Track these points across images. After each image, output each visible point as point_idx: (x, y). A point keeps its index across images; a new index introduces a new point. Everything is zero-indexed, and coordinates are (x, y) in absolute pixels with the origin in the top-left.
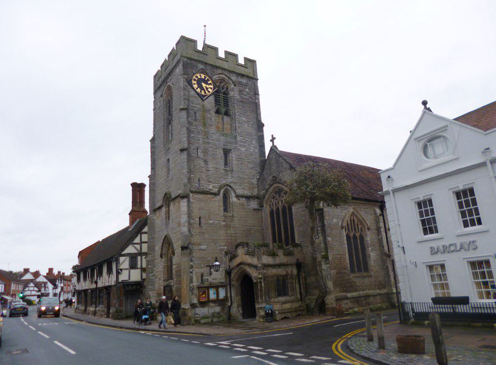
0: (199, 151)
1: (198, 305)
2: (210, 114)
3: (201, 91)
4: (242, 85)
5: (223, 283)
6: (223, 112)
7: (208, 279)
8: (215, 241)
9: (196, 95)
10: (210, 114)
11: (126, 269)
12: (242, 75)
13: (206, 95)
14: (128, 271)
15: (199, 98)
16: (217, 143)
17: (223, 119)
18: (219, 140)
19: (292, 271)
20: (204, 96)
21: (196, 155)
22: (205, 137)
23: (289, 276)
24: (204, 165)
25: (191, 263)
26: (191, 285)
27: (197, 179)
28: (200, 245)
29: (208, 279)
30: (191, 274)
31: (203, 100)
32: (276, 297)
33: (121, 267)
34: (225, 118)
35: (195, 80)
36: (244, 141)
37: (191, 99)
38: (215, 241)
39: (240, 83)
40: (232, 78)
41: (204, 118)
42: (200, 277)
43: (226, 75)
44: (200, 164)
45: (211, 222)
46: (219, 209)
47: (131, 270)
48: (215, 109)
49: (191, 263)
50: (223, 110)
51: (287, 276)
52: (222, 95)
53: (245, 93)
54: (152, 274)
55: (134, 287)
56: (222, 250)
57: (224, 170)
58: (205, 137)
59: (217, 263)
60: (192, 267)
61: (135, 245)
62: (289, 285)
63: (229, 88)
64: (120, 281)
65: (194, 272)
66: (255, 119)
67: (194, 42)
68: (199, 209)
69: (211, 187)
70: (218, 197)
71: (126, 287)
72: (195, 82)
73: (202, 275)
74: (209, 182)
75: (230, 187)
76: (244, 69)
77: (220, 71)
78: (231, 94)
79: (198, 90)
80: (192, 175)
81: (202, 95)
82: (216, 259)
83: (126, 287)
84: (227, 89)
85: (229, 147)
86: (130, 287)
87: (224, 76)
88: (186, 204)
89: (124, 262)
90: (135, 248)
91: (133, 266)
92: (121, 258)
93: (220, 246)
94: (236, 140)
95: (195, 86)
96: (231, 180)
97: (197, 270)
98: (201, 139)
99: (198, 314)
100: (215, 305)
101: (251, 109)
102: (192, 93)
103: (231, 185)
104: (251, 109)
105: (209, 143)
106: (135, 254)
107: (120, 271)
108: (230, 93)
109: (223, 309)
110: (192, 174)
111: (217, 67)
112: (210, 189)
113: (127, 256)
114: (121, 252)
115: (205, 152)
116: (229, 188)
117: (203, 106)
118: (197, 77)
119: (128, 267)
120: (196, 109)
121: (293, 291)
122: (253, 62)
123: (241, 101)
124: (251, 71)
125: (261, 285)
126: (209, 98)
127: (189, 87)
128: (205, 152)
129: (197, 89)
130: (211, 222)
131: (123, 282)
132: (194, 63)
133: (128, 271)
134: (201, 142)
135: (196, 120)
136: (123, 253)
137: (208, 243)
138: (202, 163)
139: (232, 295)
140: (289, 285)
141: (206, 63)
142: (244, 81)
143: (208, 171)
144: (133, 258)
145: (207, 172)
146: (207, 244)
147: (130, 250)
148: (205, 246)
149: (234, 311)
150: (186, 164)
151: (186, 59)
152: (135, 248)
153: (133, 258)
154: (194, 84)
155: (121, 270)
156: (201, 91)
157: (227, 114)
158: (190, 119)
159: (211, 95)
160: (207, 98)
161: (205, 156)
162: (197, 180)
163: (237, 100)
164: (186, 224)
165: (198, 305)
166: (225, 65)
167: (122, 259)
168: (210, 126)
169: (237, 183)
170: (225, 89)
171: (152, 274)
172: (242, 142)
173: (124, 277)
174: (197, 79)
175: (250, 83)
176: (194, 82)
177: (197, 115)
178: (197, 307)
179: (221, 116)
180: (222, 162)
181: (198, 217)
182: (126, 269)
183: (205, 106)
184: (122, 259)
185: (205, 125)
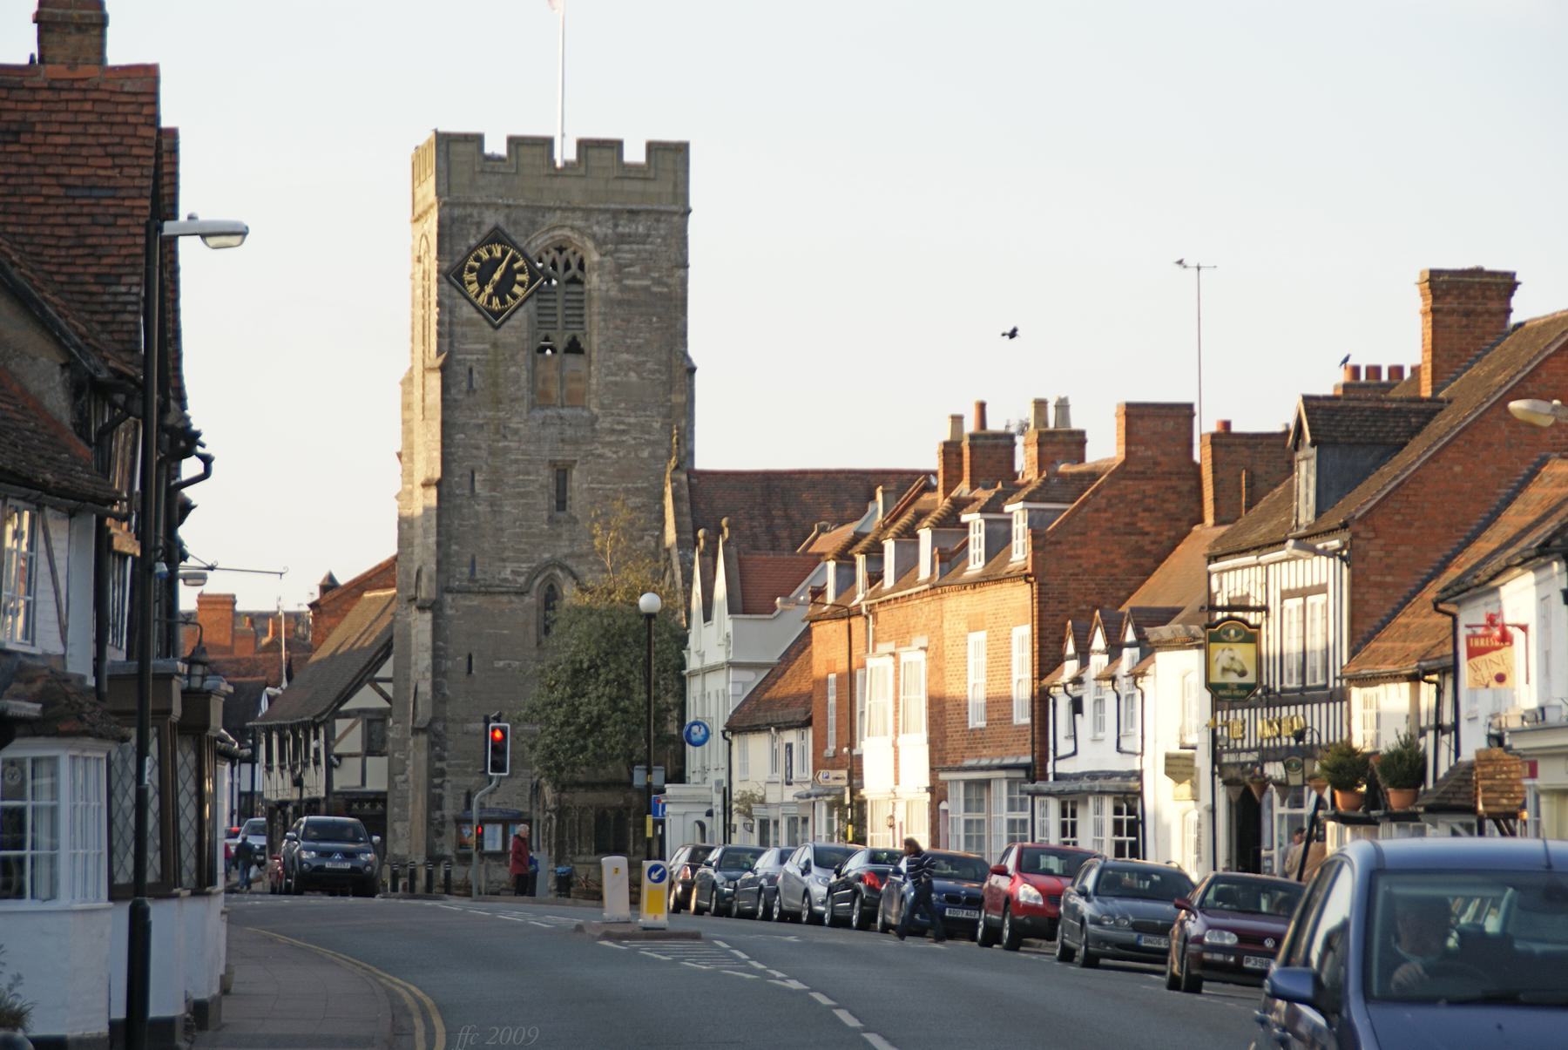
1: (454, 860)
14: (358, 761)
15: (485, 323)
20: (497, 315)
21: (467, 492)
22: (498, 437)
23: (632, 811)
25: (438, 765)
26: (438, 814)
28: (467, 721)
30: (438, 791)
31: (496, 328)
33: (338, 750)
35: (471, 270)
36: (622, 427)
39: (622, 239)
41: (495, 384)
43: (572, 228)
44: (477, 513)
45: (501, 664)
47: (369, 760)
49: (438, 765)
50: (561, 341)
51: (628, 809)
54: (402, 778)
55: (367, 806)
61: (381, 685)
62: (631, 829)
64: (336, 788)
65: (448, 786)
67: (477, 140)
69: (507, 573)
70: (527, 599)
72: (473, 276)
74: (503, 560)
75: (563, 568)
78: (594, 280)
80: (455, 547)
81: (492, 312)
84: (581, 266)
85: (565, 454)
86: (367, 806)
88: (429, 626)
89: (350, 738)
90: (382, 693)
91: (373, 746)
92: (338, 722)
94: (594, 430)
96: (566, 551)
102: (467, 311)
103: (569, 562)
106: (379, 711)
110: (456, 544)
112: (506, 580)
114: (341, 704)
115: (495, 483)
116: (558, 572)
118: (478, 259)
119: (358, 749)
120: (475, 357)
122: (679, 151)
123: (620, 303)
128: (495, 483)
130: (501, 664)
132: (471, 216)
133: (358, 761)
134: (484, 454)
138: (482, 508)
140: (631, 829)
142: (641, 229)
144: (374, 723)
147: (366, 698)
152: (382, 693)
153: (374, 723)
154: (470, 283)
155: (339, 757)
157: (574, 347)
159: (520, 305)
160: (508, 318)
161: (494, 490)
163: (609, 302)
164: (429, 675)
165: (454, 860)
169: (587, 555)
170: (574, 266)
171: (402, 778)
172: (613, 431)
173: (347, 778)
174: (477, 265)
176: (468, 277)
177: (475, 375)
180: (544, 503)
181: (466, 653)
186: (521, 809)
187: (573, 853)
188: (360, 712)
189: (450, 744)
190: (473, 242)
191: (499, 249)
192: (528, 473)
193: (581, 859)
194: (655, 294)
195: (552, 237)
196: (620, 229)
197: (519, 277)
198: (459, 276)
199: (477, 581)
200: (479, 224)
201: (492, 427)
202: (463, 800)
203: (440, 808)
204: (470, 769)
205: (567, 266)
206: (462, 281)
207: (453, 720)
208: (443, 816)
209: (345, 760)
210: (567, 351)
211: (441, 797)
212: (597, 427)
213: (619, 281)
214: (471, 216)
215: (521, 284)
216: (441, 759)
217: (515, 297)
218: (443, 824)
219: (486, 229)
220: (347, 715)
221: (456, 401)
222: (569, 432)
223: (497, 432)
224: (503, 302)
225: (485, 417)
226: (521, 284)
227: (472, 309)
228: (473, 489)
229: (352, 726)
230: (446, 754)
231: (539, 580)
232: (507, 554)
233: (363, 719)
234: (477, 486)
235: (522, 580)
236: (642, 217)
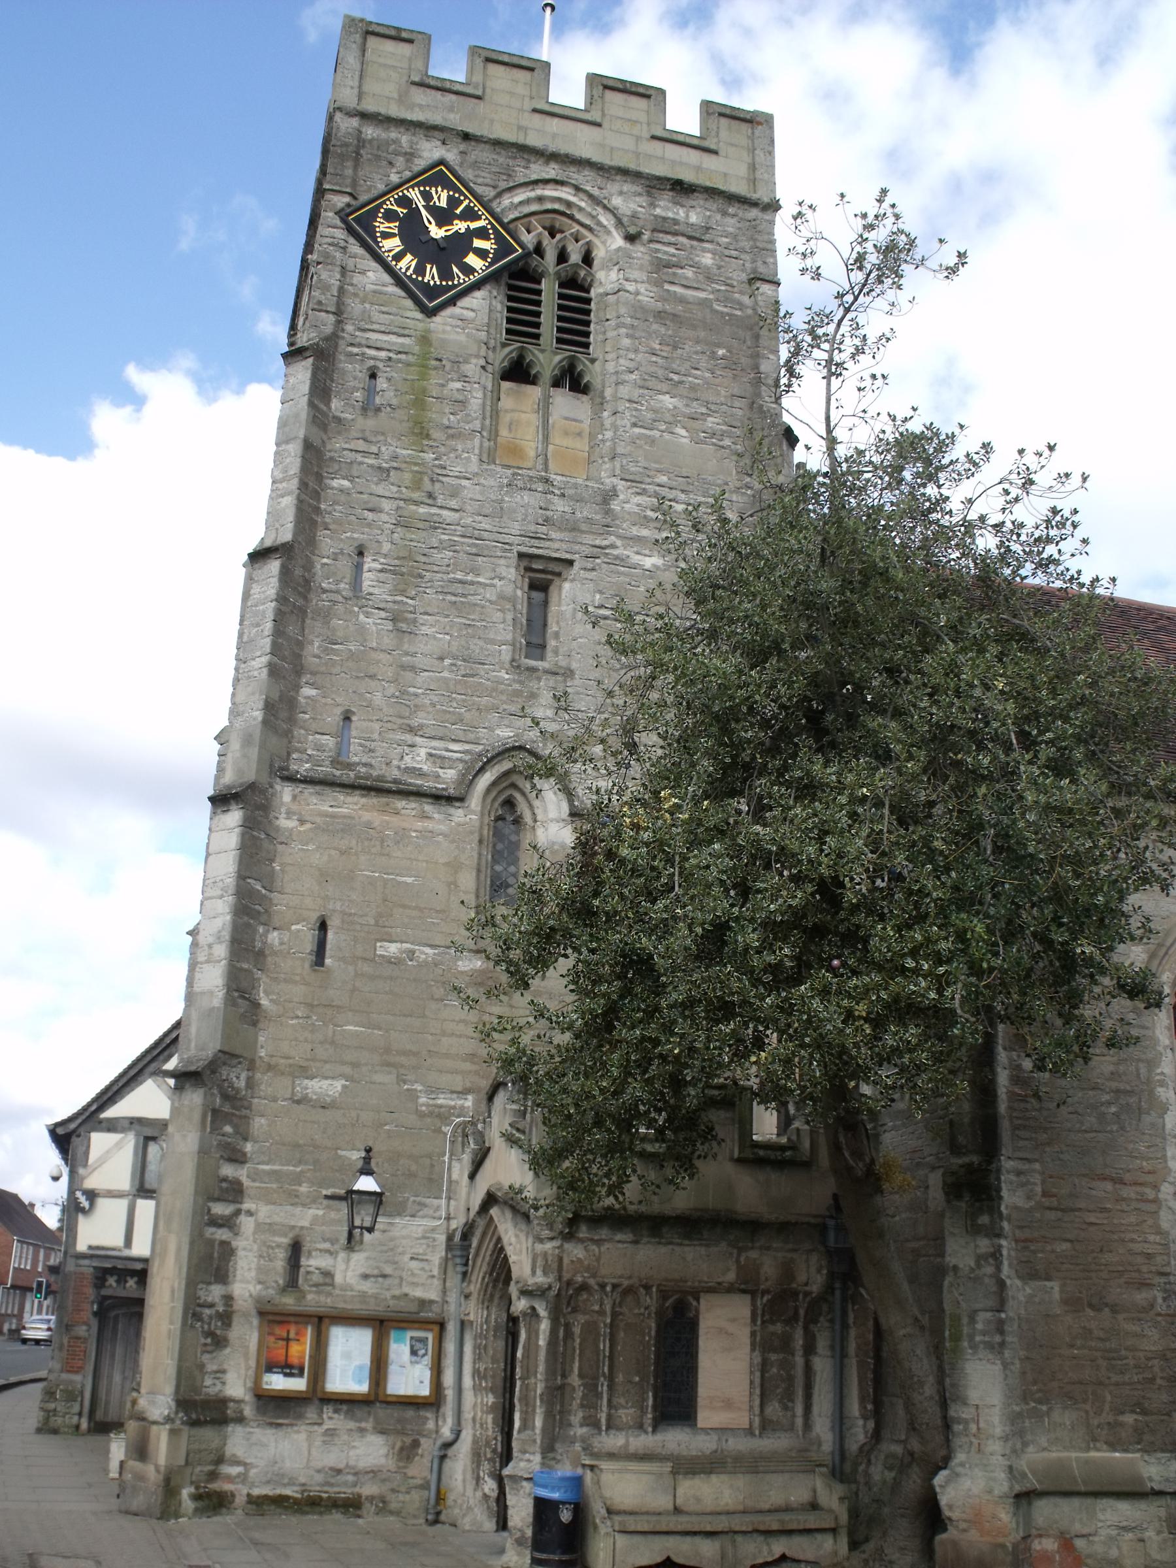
0: (369, 563)
1: (248, 1411)
2: (464, 378)
3: (420, 270)
4: (675, 234)
5: (423, 1303)
6: (547, 373)
7: (328, 1274)
8: (403, 1060)
9: (393, 289)
10: (464, 378)
11: (117, 1195)
12: (681, 188)
13: (449, 288)
14: (123, 1204)
15: (409, 303)
16: (485, 524)
17: (544, 407)
18: (499, 511)
19: (788, 1272)
20: (432, 292)
22: (416, 495)
24: (388, 641)
25: (228, 1170)
26: (215, 1292)
27: (339, 711)
28: (304, 1072)
29: (328, 1274)
30: (222, 1234)
31: (431, 313)
32: (640, 1427)
33: (89, 1184)
34: (564, 402)
35: (390, 216)
37: (354, 307)
38: (403, 1060)
39: (664, 227)
40: (617, 201)
41: (419, 402)
42: (281, 1256)
43: (577, 189)
44: (362, 630)
45: (393, 948)
46: (453, 885)
48: (501, 357)
49: (228, 1170)
52: (549, 289)
53: (689, 273)
56: (442, 1115)
57: (515, 666)
58: (416, 495)
59: (366, 1184)
60: (234, 1192)
63: (599, 254)
64: (81, 1246)
65: (247, 1224)
66: (738, 403)
68: (324, 877)
69: (419, 758)
70: (458, 814)
71: (112, 1281)
72: (393, 227)
73: (296, 1250)
74: (411, 730)
76: (693, 156)
77: (539, 170)
78: (605, 279)
79: (408, 263)
80: (307, 691)
81: (425, 287)
82: (367, 1160)
83: (112, 1281)
84: (588, 259)
85: (557, 545)
87: (565, 193)
92: (95, 1136)
93: (433, 1090)
94: (608, 512)
95: (392, 245)
97: (264, 1211)
98: (387, 505)
99: (238, 1463)
100: (352, 1425)
101: (721, 352)
102: (374, 276)
104: (721, 352)
105: (434, 525)
107: (85, 1204)
108: (600, 275)
109: (408, 1452)
110: (312, 685)
111: (524, 150)
113: (123, 1130)
117: (425, 339)
120: (383, 354)
121: (789, 1396)
123: (660, 315)
124: (742, 170)
125: (533, 1334)
126: (465, 302)
127: (355, 248)
129: (398, 257)
130: (393, 948)
131: (95, 1254)
133: (123, 1204)
134: (386, 519)
135: (368, 408)
136: (111, 1113)
137: (355, 1065)
138: (374, 623)
139: (468, 1381)
141: (466, 137)
142: (693, 218)
143: (413, 669)
145: (409, 675)
146: (347, 1070)
148: (338, 1085)
149: (459, 1476)
150: (268, 626)
151: (355, 122)
154: (386, 236)
155: (92, 1195)
156: (420, 270)
158: (335, 404)
160: (452, 302)
161: (403, 593)
162: (332, 718)
163: (640, 312)
165: (248, 1411)
166: (582, 141)
167: (100, 1141)
168: (452, 436)
170: (575, 257)
175: (729, 223)
176: (382, 226)
178: (240, 1420)
179: (534, 393)
181: (314, 916)
182: (117, 1195)
183: (433, 337)
184: (100, 1141)
185: (420, 433)
186: (418, 1293)
187: (592, 1422)
188: (135, 1122)
189: (259, 1124)
190: (395, 178)
191: (444, 195)
192: (476, 571)
193: (614, 1441)
194: (717, 311)
195: (540, 199)
196: (658, 211)
197: (478, 243)
198: (367, 222)
199: (350, 766)
200: (410, 156)
201: (407, 476)
202: (280, 1262)
203: (222, 1275)
204: (304, 1189)
205: (562, 257)
206: (371, 231)
207: (270, 1067)
208: (228, 1299)
209: (101, 1203)
210: (557, 383)
211: (227, 1251)
212: (615, 506)
213: (658, 283)
214: (394, 141)
215: (482, 254)
216: (237, 1158)
217: (468, 270)
218: (226, 1318)
219: (420, 164)
220: (112, 1126)
221: (339, 420)
222: (560, 506)
223: (417, 485)
224: (445, 274)
225: (395, 457)
226: (482, 254)
227: (387, 278)
228: (356, 583)
229: (119, 1145)
230: (249, 1147)
231: (487, 778)
232: (419, 719)
233: (137, 1135)
234: (368, 580)
235: (450, 774)
236: (698, 200)
